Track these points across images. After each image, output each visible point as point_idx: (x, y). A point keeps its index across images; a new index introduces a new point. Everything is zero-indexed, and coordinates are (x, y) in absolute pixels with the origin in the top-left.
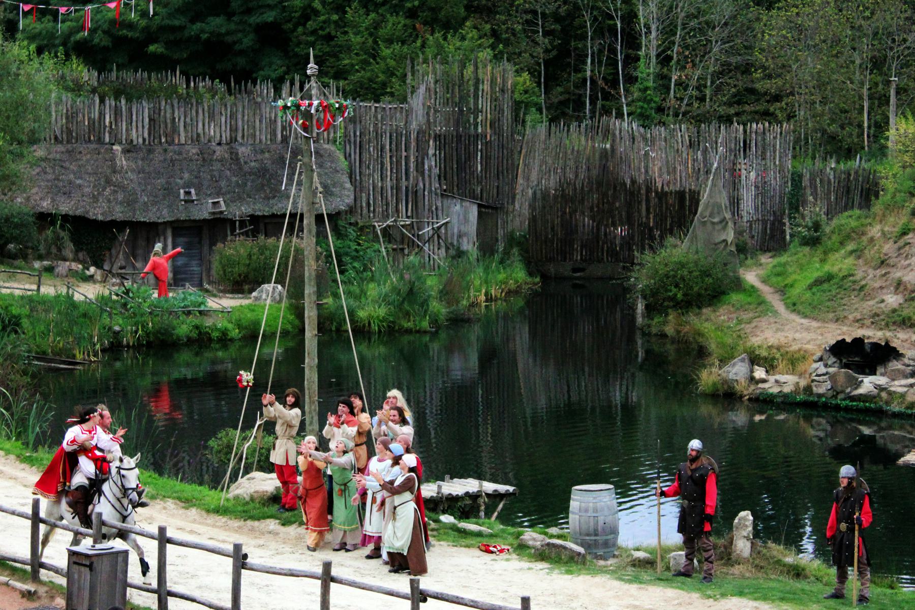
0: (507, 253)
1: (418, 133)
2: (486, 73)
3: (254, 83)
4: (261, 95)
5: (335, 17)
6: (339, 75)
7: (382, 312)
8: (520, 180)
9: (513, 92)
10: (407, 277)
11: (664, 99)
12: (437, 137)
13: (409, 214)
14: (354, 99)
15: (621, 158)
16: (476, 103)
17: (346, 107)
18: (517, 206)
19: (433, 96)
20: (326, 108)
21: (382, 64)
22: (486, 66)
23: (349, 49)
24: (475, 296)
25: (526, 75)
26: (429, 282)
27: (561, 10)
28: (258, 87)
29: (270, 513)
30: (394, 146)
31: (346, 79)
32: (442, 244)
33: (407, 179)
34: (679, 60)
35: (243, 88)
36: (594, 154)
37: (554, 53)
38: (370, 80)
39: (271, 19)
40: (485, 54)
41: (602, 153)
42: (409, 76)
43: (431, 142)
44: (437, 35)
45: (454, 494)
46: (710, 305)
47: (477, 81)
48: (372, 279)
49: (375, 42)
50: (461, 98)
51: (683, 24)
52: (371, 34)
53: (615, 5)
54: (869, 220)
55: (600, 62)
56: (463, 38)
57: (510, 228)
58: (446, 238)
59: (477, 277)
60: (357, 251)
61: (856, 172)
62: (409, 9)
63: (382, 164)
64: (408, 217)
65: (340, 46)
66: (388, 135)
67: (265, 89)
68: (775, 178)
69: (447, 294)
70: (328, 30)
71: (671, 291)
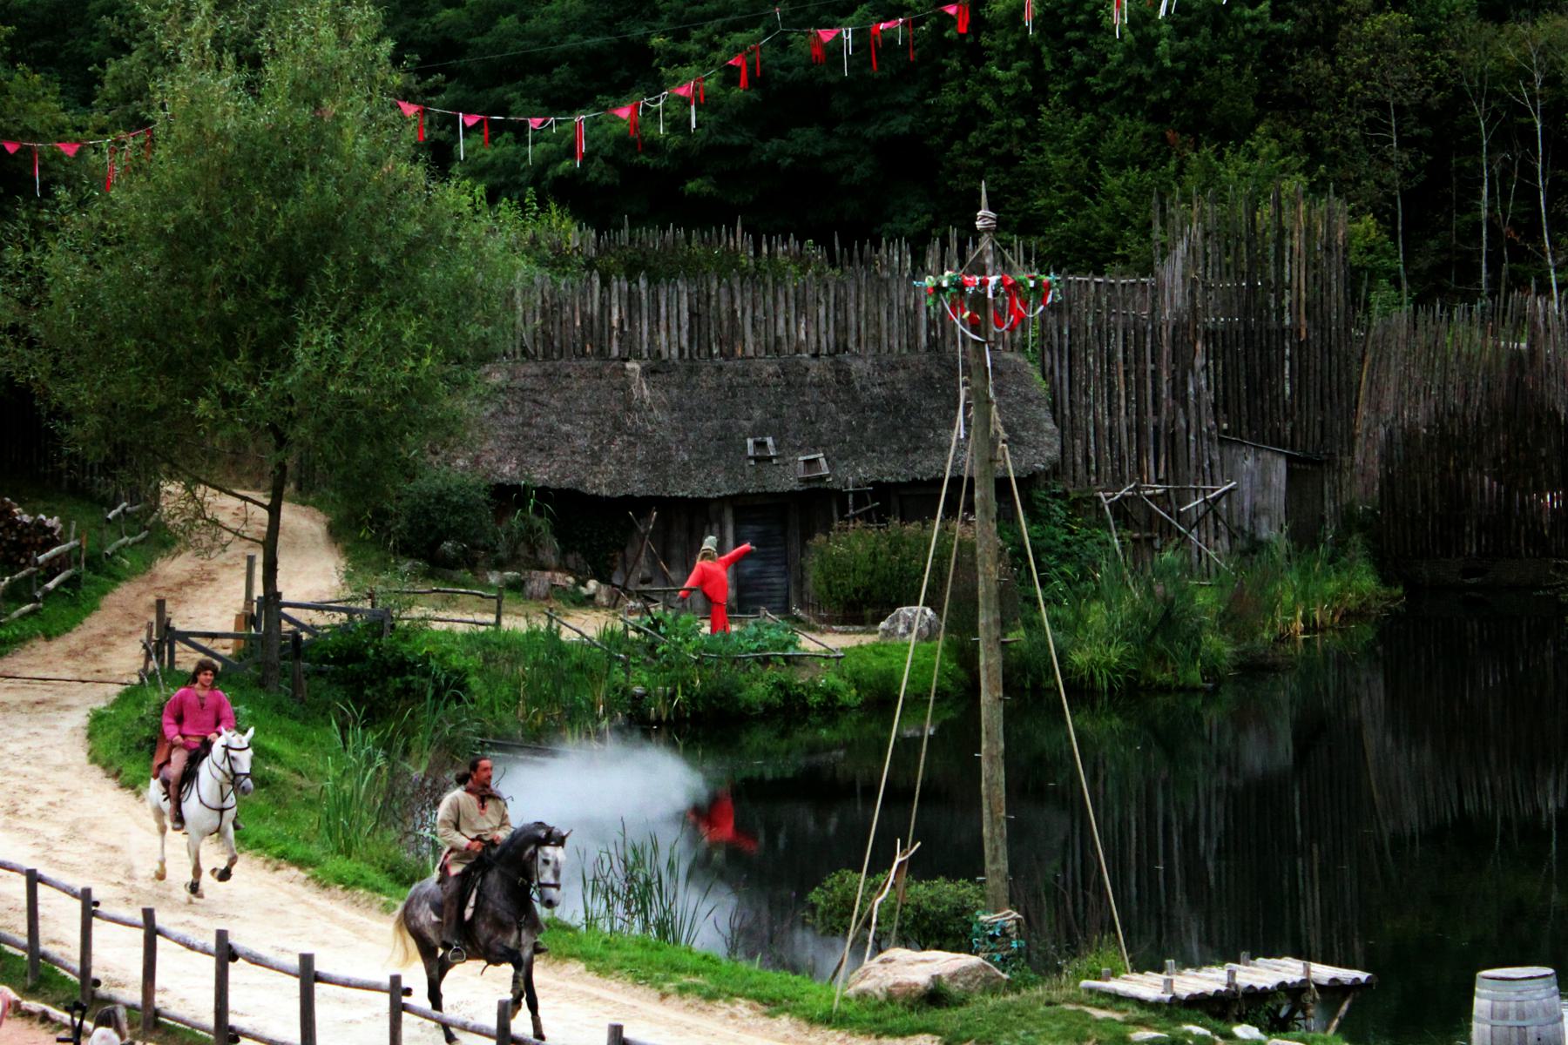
0: (1340, 544)
1: (1175, 328)
2: (1297, 218)
3: (877, 246)
4: (889, 266)
5: (1020, 123)
6: (1029, 226)
7: (1114, 654)
8: (1363, 411)
9: (1346, 251)
10: (1159, 589)
12: (1210, 336)
13: (1162, 475)
14: (1057, 271)
15: (1548, 366)
16: (1280, 274)
18: (1358, 459)
19: (1201, 262)
21: (1107, 205)
22: (1296, 205)
23: (1045, 179)
24: (1285, 623)
25: (1369, 220)
26: (1200, 600)
27: (1430, 100)
28: (883, 251)
29: (921, 1024)
30: (1131, 354)
31: (1041, 233)
32: (1223, 529)
33: (1157, 412)
35: (856, 254)
36: (1498, 364)
37: (1421, 177)
38: (1085, 234)
39: (905, 129)
40: (1294, 184)
41: (1511, 360)
42: (1157, 227)
43: (1199, 346)
44: (1205, 151)
45: (1259, 985)
47: (1282, 233)
48: (1097, 595)
49: (1093, 166)
50: (1251, 263)
52: (1085, 153)
53: (1531, 89)
55: (1505, 195)
56: (1253, 156)
57: (1346, 499)
58: (1230, 517)
59: (1287, 589)
60: (1067, 543)
62: (1155, 106)
63: (1111, 386)
64: (1159, 481)
65: (1030, 174)
66: (1121, 334)
67: (897, 256)
69: (1233, 620)
70: (1007, 146)
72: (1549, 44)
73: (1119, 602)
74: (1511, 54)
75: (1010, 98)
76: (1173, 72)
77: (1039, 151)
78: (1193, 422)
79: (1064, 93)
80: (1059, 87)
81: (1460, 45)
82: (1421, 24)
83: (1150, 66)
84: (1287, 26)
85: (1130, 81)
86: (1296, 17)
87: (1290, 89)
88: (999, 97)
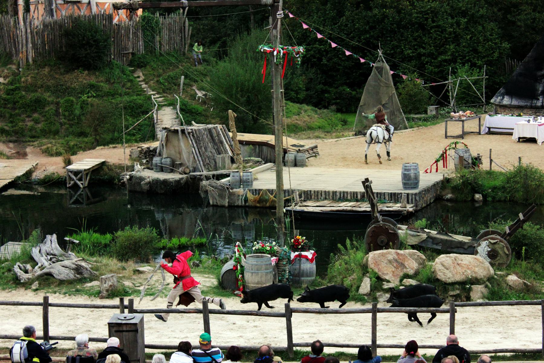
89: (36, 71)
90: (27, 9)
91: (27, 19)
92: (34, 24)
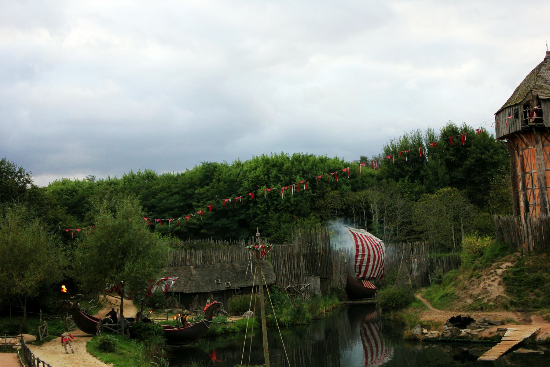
0: (331, 294)
3: (239, 241)
5: (265, 216)
6: (268, 235)
7: (289, 318)
8: (334, 268)
10: (297, 305)
11: (382, 236)
12: (304, 255)
13: (296, 283)
14: (274, 244)
17: (271, 247)
18: (334, 277)
20: (264, 248)
21: (283, 231)
22: (319, 229)
23: (270, 226)
24: (322, 310)
28: (240, 242)
31: (270, 237)
32: (309, 293)
33: (294, 270)
34: (386, 222)
35: (234, 243)
38: (279, 236)
39: (243, 218)
43: (302, 257)
44: (301, 219)
46: (405, 308)
47: (316, 234)
48: (285, 307)
49: (280, 223)
50: (311, 240)
51: (387, 209)
52: (278, 221)
53: (362, 204)
54: (458, 273)
56: (310, 220)
57: (332, 285)
58: (310, 290)
60: (278, 297)
61: (452, 257)
64: (295, 284)
65: (267, 226)
67: (242, 242)
68: (424, 261)
69: (312, 310)
70: (263, 220)
71: (391, 304)
72: (365, 195)
73: (289, 308)
74: (358, 198)
75: (263, 211)
76: (294, 204)
77: (269, 221)
78: (301, 272)
79: (273, 209)
80: (272, 208)
81: (348, 196)
82: (341, 193)
83: (289, 203)
84: (315, 194)
85: (286, 206)
86: (317, 193)
87: (316, 206)
88: (260, 211)
89: (536, 257)
90: (527, 210)
91: (527, 217)
92: (533, 221)
